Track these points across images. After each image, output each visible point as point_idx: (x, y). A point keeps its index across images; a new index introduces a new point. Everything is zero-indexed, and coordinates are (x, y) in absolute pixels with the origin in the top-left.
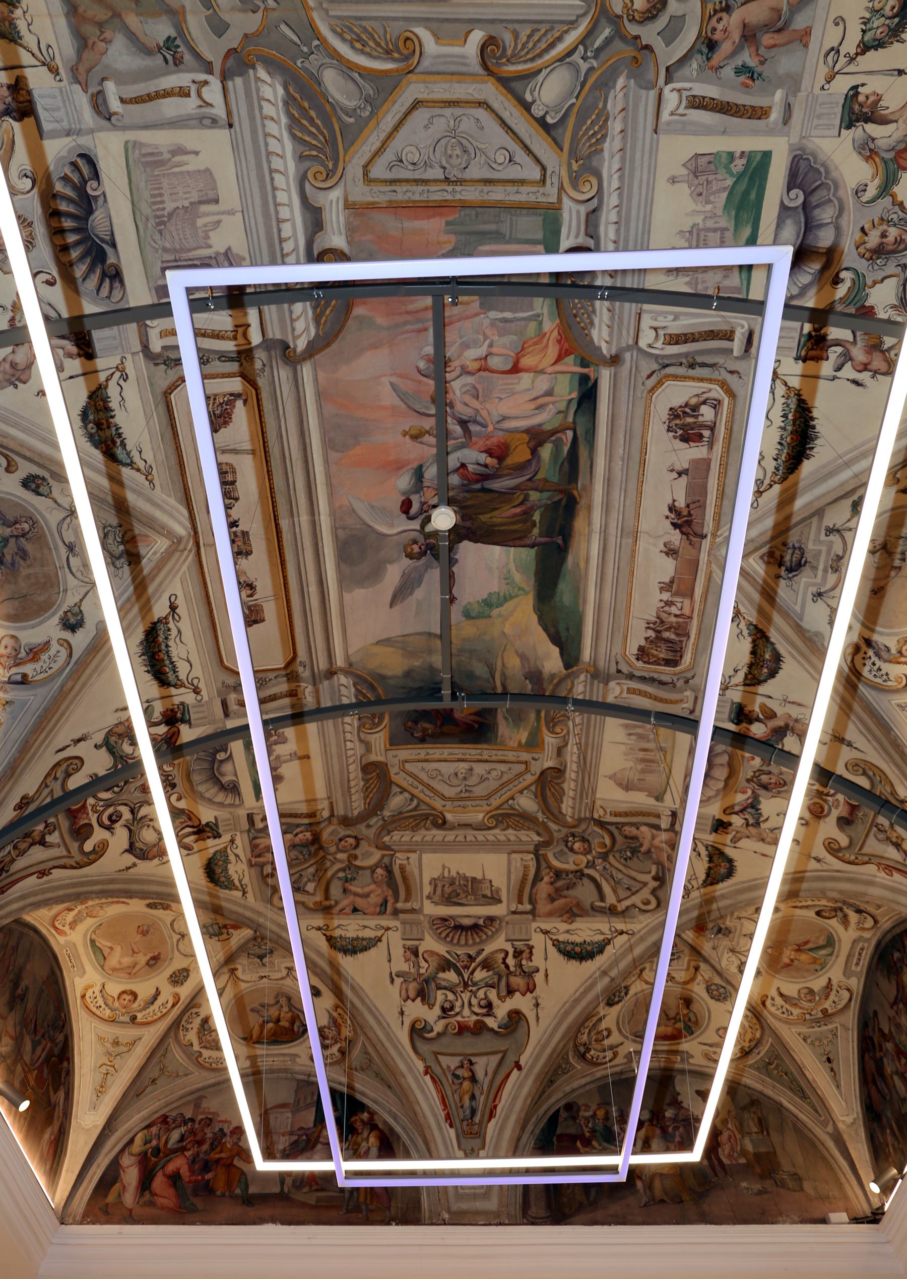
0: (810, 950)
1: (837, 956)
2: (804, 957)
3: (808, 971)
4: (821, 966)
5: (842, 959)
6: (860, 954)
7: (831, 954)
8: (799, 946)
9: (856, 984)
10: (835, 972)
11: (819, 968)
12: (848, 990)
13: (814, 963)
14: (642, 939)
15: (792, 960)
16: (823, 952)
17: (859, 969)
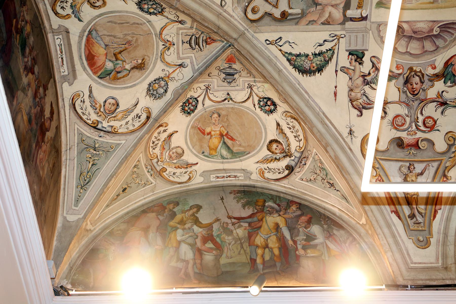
0: (224, 143)
1: (223, 163)
2: (215, 141)
3: (201, 147)
4: (210, 153)
5: (221, 166)
6: (229, 176)
7: (223, 157)
8: (227, 134)
9: (198, 181)
10: (204, 165)
11: (206, 154)
12: (190, 179)
13: (211, 149)
14: (219, 15)
15: (209, 134)
16: (224, 152)
17: (214, 179)
